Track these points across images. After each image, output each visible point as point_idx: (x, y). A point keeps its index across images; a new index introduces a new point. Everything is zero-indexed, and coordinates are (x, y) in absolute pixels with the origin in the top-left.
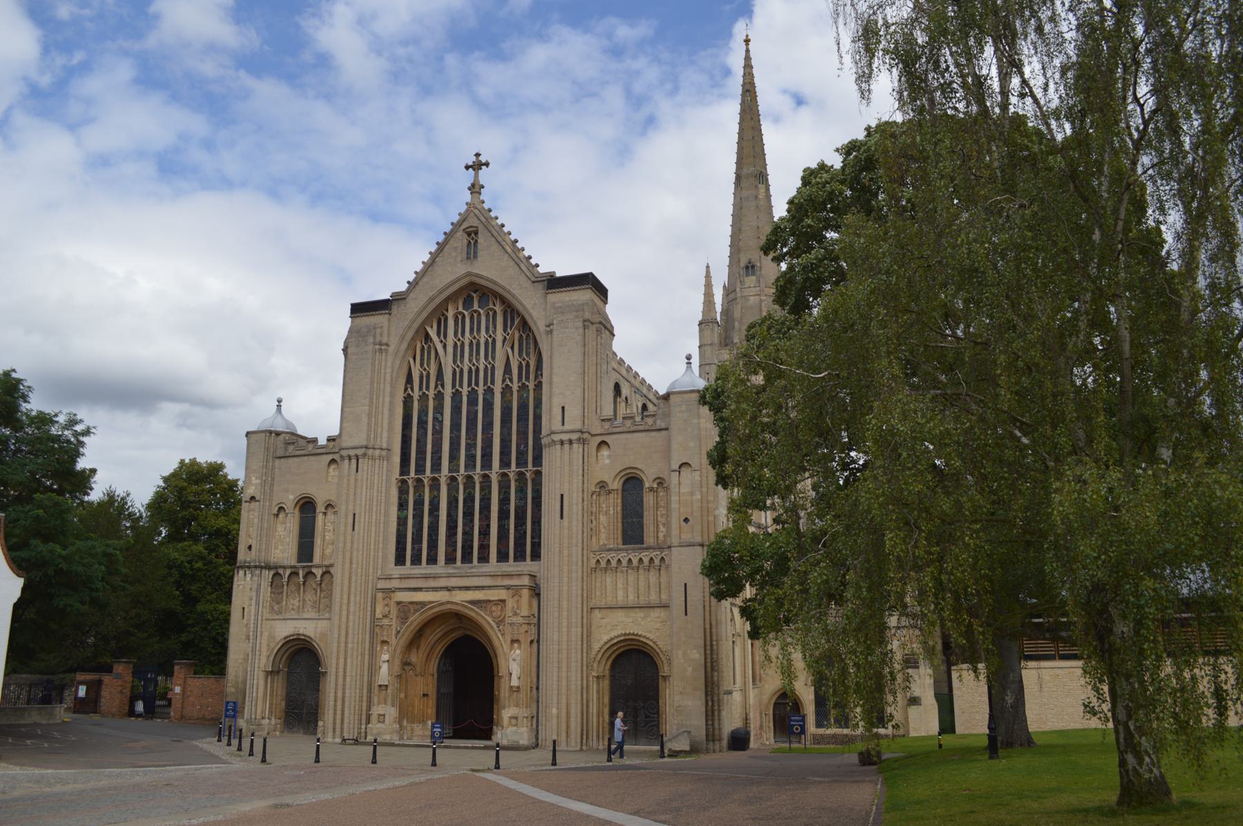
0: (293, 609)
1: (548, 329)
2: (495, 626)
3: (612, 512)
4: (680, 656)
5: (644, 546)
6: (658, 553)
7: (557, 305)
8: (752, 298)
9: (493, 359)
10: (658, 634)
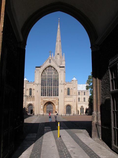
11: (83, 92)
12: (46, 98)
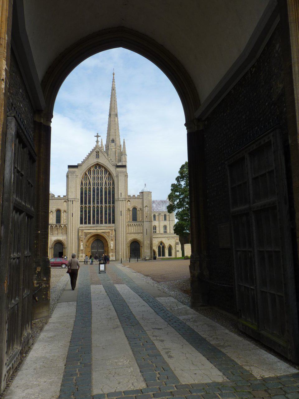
9: (102, 180)
11: (163, 214)
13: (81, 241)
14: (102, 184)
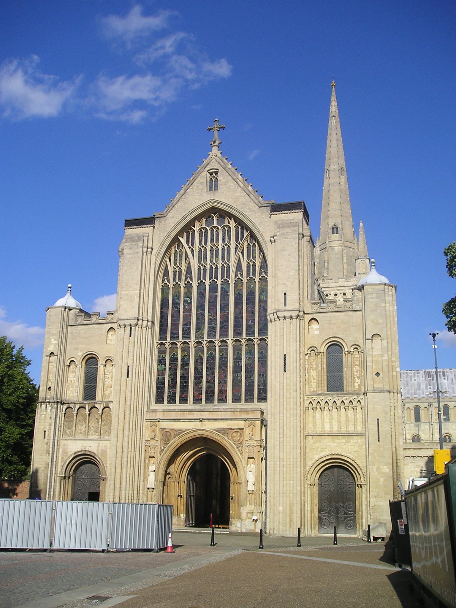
0: (80, 433)
1: (272, 239)
2: (236, 447)
3: (320, 368)
4: (375, 470)
5: (344, 392)
6: (356, 397)
7: (279, 223)
8: (336, 248)
9: (229, 260)
10: (356, 455)
12: (191, 411)
13: (150, 457)
14: (226, 269)
